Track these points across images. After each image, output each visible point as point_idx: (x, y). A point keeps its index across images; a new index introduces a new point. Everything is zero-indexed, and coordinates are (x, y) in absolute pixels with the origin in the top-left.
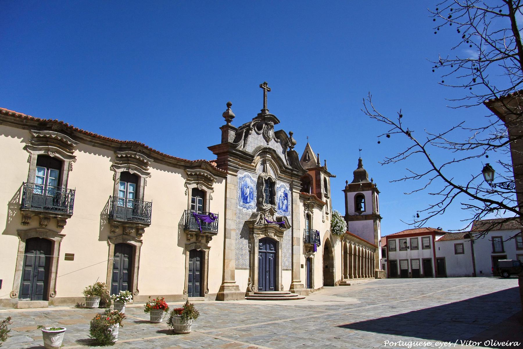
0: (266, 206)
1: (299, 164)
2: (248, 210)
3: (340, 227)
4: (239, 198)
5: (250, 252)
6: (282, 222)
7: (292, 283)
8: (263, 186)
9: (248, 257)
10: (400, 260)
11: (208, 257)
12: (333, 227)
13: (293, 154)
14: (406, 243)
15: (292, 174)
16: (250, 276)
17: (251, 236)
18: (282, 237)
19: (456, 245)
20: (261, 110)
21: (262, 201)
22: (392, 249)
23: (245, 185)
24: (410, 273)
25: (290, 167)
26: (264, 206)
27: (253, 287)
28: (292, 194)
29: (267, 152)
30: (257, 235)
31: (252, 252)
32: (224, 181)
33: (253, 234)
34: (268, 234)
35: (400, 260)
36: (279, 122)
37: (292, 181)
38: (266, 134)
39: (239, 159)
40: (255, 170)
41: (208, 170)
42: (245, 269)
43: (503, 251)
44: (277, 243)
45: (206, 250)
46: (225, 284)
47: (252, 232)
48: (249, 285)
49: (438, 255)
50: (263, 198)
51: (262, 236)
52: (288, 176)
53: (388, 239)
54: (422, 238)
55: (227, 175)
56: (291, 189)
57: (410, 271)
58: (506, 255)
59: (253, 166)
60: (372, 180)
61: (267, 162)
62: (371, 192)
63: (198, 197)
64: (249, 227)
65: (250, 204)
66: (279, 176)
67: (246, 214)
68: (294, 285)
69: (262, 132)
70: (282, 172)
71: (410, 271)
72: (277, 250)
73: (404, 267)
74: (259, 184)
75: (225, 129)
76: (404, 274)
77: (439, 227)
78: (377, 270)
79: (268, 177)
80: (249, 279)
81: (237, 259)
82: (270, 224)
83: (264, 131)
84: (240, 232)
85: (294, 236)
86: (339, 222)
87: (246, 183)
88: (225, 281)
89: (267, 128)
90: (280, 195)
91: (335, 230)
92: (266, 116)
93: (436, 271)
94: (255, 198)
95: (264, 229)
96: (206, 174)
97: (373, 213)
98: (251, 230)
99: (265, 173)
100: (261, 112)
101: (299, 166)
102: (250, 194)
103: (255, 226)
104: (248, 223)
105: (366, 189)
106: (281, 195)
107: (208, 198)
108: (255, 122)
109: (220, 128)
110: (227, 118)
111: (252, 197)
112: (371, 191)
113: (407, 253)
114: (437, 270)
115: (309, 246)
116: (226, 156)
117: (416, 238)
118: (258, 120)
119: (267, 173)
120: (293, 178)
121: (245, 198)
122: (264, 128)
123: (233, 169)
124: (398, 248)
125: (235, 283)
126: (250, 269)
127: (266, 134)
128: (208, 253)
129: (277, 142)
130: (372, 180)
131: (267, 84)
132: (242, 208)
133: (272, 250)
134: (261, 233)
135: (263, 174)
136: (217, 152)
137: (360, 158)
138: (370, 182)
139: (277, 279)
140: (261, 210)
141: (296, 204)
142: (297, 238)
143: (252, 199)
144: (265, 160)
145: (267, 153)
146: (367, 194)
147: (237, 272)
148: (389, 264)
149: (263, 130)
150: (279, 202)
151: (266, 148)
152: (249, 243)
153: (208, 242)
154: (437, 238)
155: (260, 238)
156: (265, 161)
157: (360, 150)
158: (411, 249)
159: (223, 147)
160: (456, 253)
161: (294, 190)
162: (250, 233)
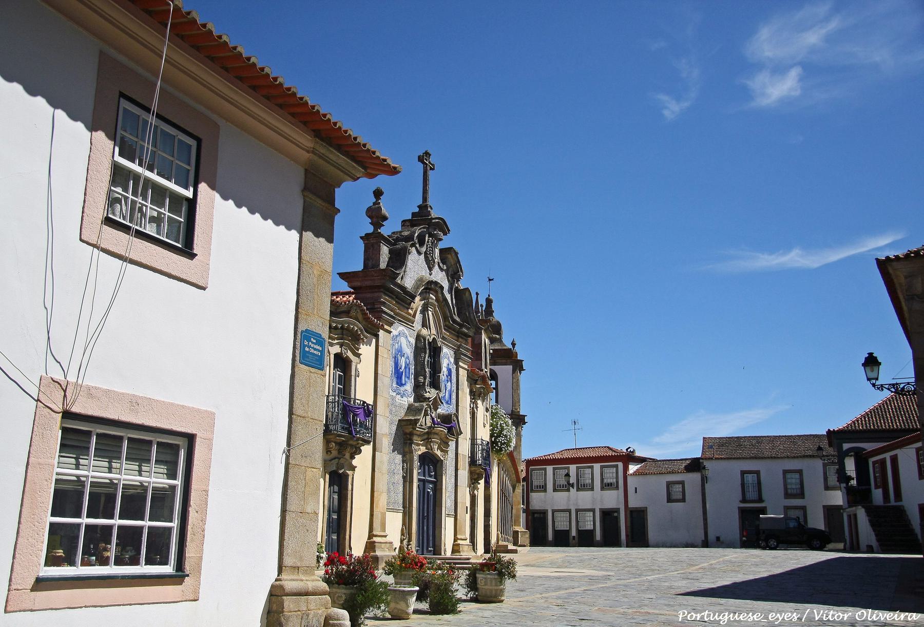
0: (429, 392)
1: (472, 315)
2: (402, 399)
3: (508, 437)
5: (404, 477)
6: (452, 424)
7: (454, 542)
8: (425, 353)
9: (401, 489)
10: (554, 511)
11: (352, 485)
12: (494, 436)
13: (465, 294)
14: (568, 475)
15: (458, 333)
16: (404, 524)
17: (407, 449)
18: (447, 452)
19: (669, 484)
20: (418, 207)
21: (424, 383)
22: (608, 486)
24: (574, 537)
25: (458, 319)
26: (426, 392)
27: (410, 546)
28: (457, 371)
29: (430, 289)
31: (407, 479)
32: (374, 340)
33: (411, 444)
34: (431, 446)
35: (554, 511)
36: (449, 233)
37: (459, 347)
38: (430, 253)
39: (396, 302)
40: (413, 324)
41: (357, 319)
42: (396, 511)
43: (760, 500)
44: (440, 463)
45: (350, 473)
46: (375, 539)
47: (409, 442)
48: (402, 541)
49: (632, 504)
50: (425, 379)
51: (423, 449)
53: (531, 467)
54: (602, 467)
56: (456, 363)
57: (574, 533)
58: (766, 507)
59: (410, 314)
60: (513, 344)
62: (510, 368)
63: (338, 371)
64: (403, 431)
66: (443, 337)
67: (401, 406)
68: (459, 544)
69: (424, 249)
70: (448, 328)
71: (574, 533)
72: (439, 478)
73: (562, 525)
74: (418, 350)
75: (372, 241)
76: (562, 540)
77: (630, 448)
78: (517, 528)
79: (432, 338)
80: (402, 530)
81: (389, 491)
83: (427, 249)
85: (460, 451)
86: (505, 428)
88: (375, 533)
89: (432, 243)
91: (499, 443)
92: (434, 221)
93: (627, 536)
95: (426, 437)
97: (512, 411)
98: (408, 436)
99: (427, 328)
100: (417, 210)
101: (472, 318)
102: (405, 367)
103: (417, 429)
104: (404, 423)
105: (500, 361)
107: (353, 373)
108: (420, 231)
109: (361, 238)
110: (375, 220)
111: (408, 375)
112: (512, 366)
113: (569, 498)
114: (629, 534)
115: (478, 471)
116: (376, 295)
117: (565, 468)
118: (424, 228)
119: (430, 329)
120: (460, 340)
122: (428, 242)
124: (550, 486)
125: (385, 536)
126: (404, 511)
127: (430, 253)
128: (353, 478)
129: (441, 269)
130: (513, 344)
131: (430, 155)
132: (394, 394)
133: (430, 476)
134: (421, 443)
135: (425, 332)
136: (358, 284)
137: (489, 296)
138: (511, 347)
139: (437, 532)
140: (421, 399)
142: (463, 455)
143: (408, 378)
144: (427, 304)
145: (431, 292)
146: (504, 371)
148: (530, 517)
149: (425, 246)
151: (431, 282)
152: (403, 461)
153: (353, 457)
154: (633, 468)
155: (420, 453)
156: (426, 306)
157: (490, 280)
158: (578, 490)
159: (373, 276)
160: (670, 500)
161: (460, 363)
162: (405, 443)
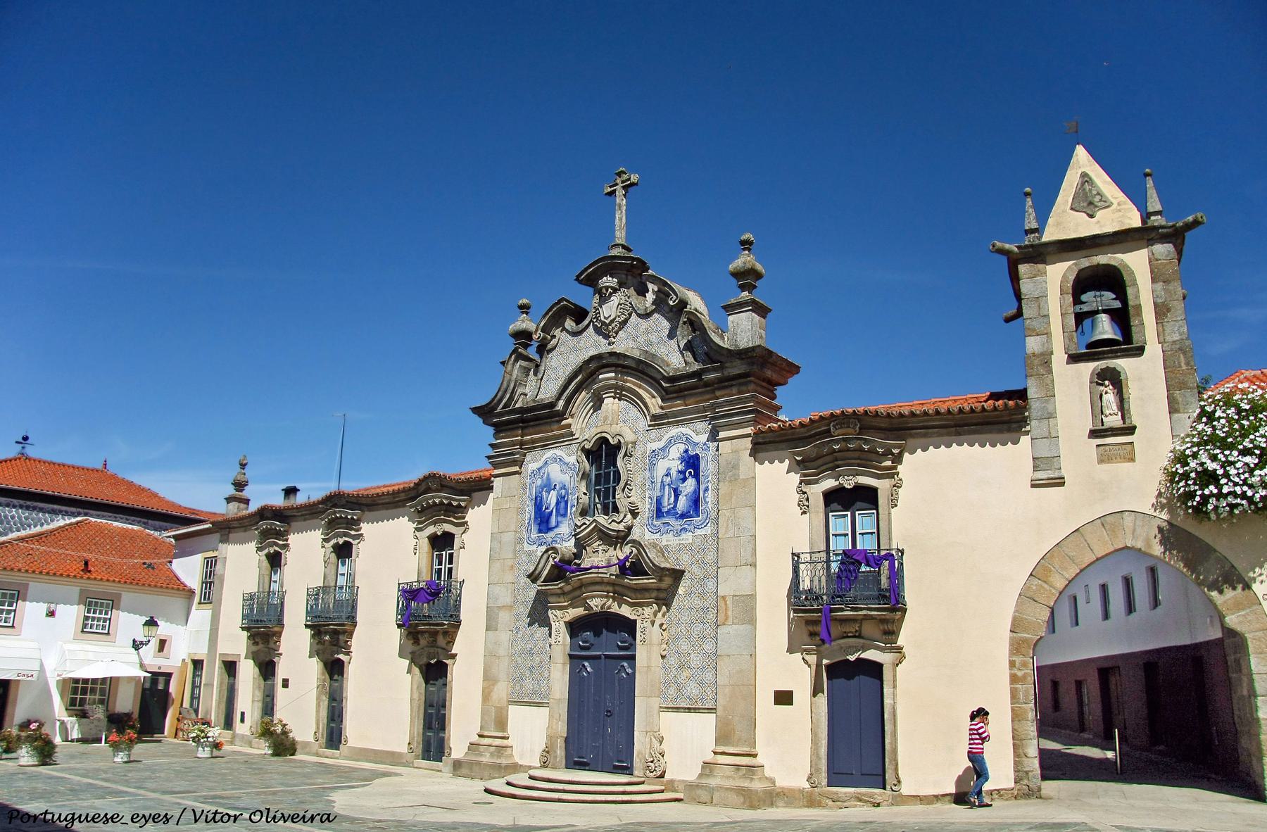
4: (528, 523)
23: (545, 487)
30: (558, 613)
52: (700, 398)
55: (492, 482)
61: (604, 396)
65: (557, 531)
82: (578, 575)
84: (528, 610)
87: (549, 479)
90: (664, 472)
94: (571, 510)
96: (437, 501)
102: (558, 503)
106: (669, 469)
111: (562, 511)
120: (718, 393)
121: (546, 518)
123: (502, 462)
141: (735, 479)
147: (516, 714)
150: (659, 494)
155: (567, 619)
